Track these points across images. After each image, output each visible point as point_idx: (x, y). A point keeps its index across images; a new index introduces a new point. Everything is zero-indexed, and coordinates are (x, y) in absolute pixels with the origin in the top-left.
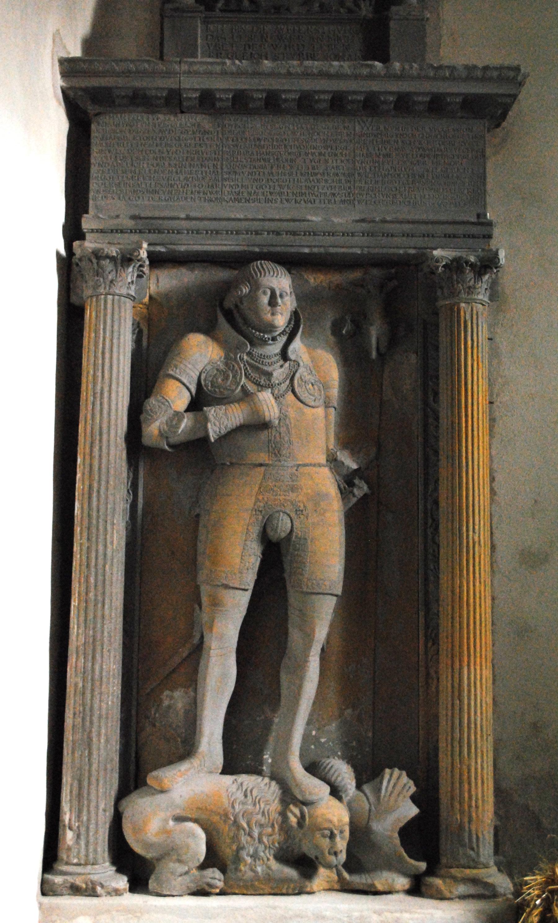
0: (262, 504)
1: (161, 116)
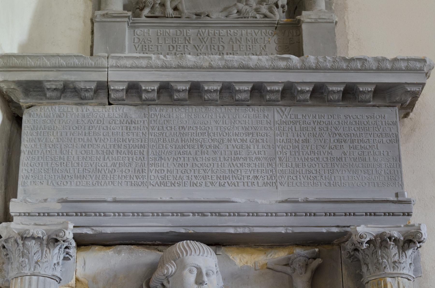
1: (90, 108)
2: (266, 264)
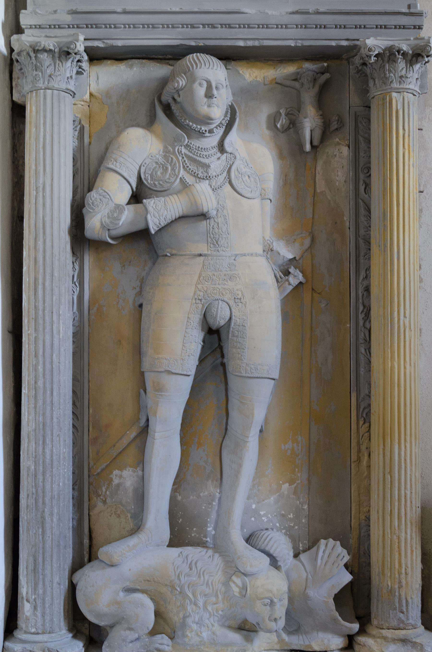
0: (201, 294)
2: (275, 79)
